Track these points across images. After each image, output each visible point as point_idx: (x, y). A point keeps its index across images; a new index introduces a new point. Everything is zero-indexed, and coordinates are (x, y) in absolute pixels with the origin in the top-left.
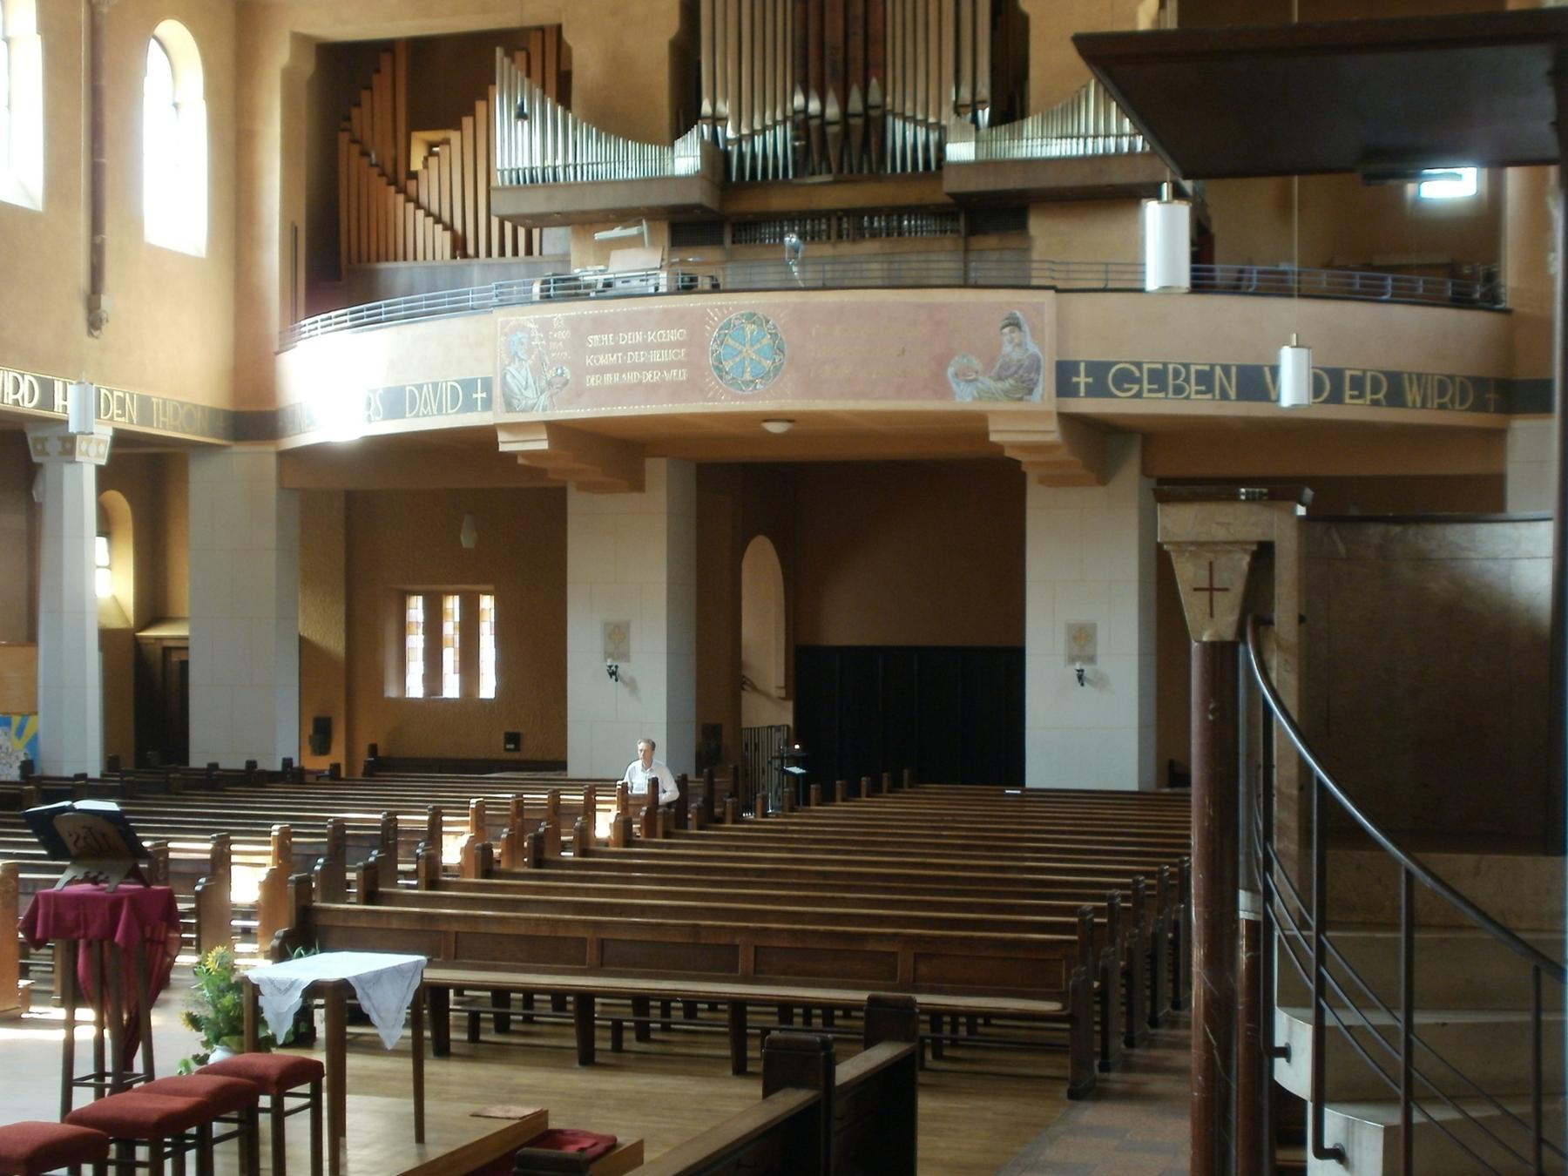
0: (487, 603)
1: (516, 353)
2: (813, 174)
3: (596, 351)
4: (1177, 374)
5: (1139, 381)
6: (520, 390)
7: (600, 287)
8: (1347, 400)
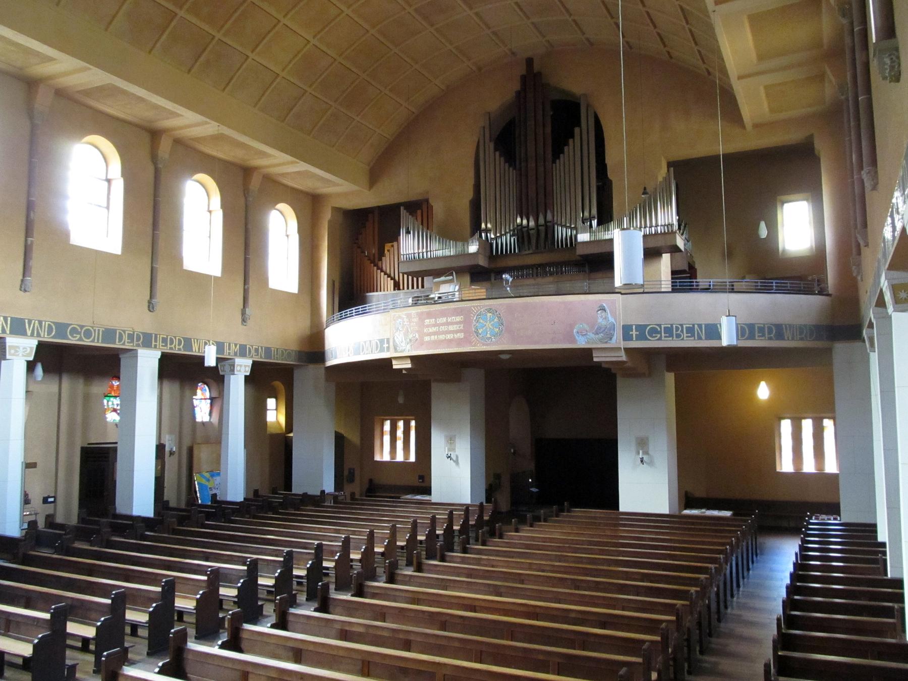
0: (413, 423)
2: (525, 250)
3: (428, 326)
4: (677, 329)
5: (660, 333)
7: (436, 299)
8: (757, 338)
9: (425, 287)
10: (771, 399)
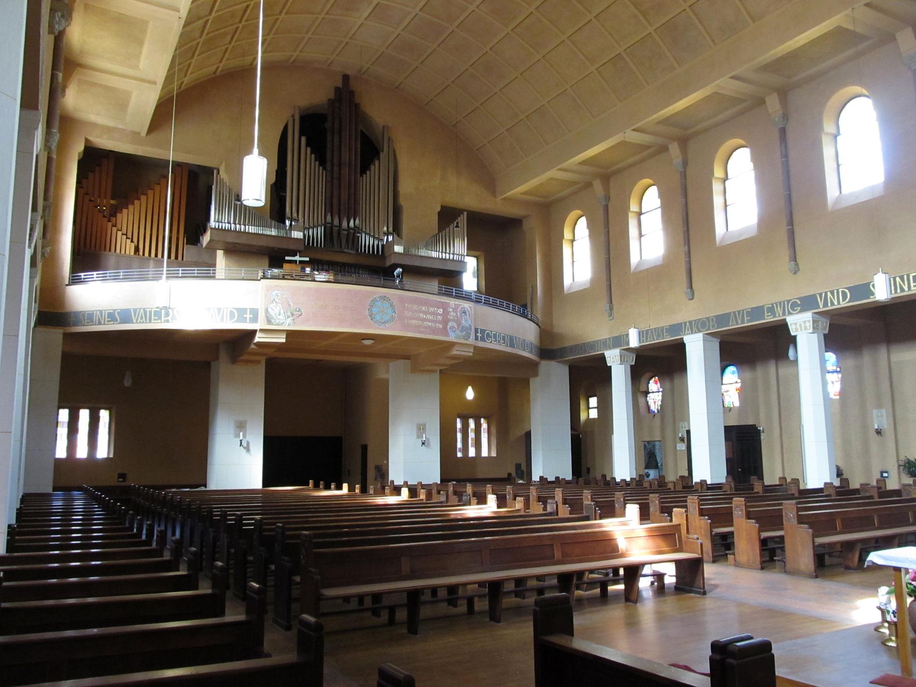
0: (104, 415)
1: (274, 299)
4: (499, 336)
6: (276, 316)
9: (184, 260)
10: (475, 398)
